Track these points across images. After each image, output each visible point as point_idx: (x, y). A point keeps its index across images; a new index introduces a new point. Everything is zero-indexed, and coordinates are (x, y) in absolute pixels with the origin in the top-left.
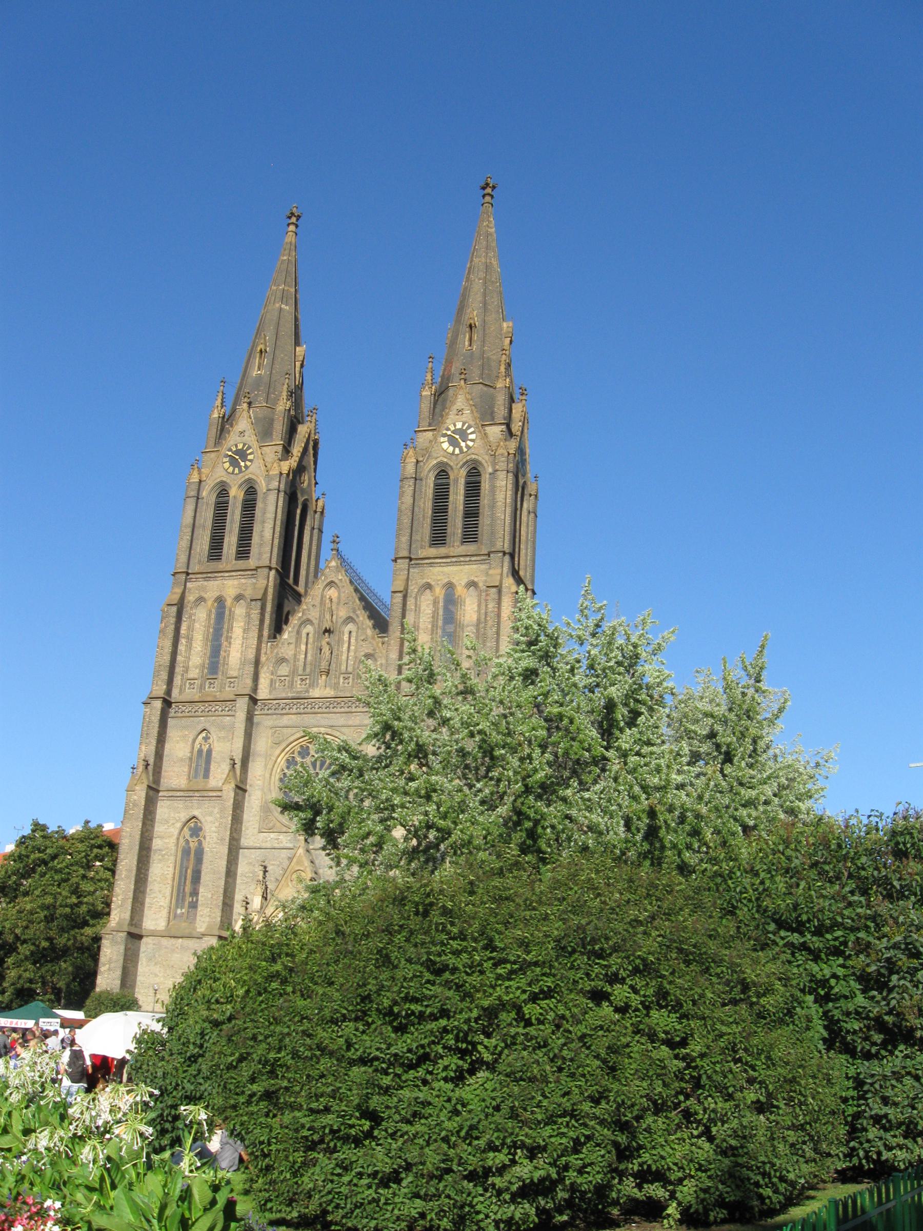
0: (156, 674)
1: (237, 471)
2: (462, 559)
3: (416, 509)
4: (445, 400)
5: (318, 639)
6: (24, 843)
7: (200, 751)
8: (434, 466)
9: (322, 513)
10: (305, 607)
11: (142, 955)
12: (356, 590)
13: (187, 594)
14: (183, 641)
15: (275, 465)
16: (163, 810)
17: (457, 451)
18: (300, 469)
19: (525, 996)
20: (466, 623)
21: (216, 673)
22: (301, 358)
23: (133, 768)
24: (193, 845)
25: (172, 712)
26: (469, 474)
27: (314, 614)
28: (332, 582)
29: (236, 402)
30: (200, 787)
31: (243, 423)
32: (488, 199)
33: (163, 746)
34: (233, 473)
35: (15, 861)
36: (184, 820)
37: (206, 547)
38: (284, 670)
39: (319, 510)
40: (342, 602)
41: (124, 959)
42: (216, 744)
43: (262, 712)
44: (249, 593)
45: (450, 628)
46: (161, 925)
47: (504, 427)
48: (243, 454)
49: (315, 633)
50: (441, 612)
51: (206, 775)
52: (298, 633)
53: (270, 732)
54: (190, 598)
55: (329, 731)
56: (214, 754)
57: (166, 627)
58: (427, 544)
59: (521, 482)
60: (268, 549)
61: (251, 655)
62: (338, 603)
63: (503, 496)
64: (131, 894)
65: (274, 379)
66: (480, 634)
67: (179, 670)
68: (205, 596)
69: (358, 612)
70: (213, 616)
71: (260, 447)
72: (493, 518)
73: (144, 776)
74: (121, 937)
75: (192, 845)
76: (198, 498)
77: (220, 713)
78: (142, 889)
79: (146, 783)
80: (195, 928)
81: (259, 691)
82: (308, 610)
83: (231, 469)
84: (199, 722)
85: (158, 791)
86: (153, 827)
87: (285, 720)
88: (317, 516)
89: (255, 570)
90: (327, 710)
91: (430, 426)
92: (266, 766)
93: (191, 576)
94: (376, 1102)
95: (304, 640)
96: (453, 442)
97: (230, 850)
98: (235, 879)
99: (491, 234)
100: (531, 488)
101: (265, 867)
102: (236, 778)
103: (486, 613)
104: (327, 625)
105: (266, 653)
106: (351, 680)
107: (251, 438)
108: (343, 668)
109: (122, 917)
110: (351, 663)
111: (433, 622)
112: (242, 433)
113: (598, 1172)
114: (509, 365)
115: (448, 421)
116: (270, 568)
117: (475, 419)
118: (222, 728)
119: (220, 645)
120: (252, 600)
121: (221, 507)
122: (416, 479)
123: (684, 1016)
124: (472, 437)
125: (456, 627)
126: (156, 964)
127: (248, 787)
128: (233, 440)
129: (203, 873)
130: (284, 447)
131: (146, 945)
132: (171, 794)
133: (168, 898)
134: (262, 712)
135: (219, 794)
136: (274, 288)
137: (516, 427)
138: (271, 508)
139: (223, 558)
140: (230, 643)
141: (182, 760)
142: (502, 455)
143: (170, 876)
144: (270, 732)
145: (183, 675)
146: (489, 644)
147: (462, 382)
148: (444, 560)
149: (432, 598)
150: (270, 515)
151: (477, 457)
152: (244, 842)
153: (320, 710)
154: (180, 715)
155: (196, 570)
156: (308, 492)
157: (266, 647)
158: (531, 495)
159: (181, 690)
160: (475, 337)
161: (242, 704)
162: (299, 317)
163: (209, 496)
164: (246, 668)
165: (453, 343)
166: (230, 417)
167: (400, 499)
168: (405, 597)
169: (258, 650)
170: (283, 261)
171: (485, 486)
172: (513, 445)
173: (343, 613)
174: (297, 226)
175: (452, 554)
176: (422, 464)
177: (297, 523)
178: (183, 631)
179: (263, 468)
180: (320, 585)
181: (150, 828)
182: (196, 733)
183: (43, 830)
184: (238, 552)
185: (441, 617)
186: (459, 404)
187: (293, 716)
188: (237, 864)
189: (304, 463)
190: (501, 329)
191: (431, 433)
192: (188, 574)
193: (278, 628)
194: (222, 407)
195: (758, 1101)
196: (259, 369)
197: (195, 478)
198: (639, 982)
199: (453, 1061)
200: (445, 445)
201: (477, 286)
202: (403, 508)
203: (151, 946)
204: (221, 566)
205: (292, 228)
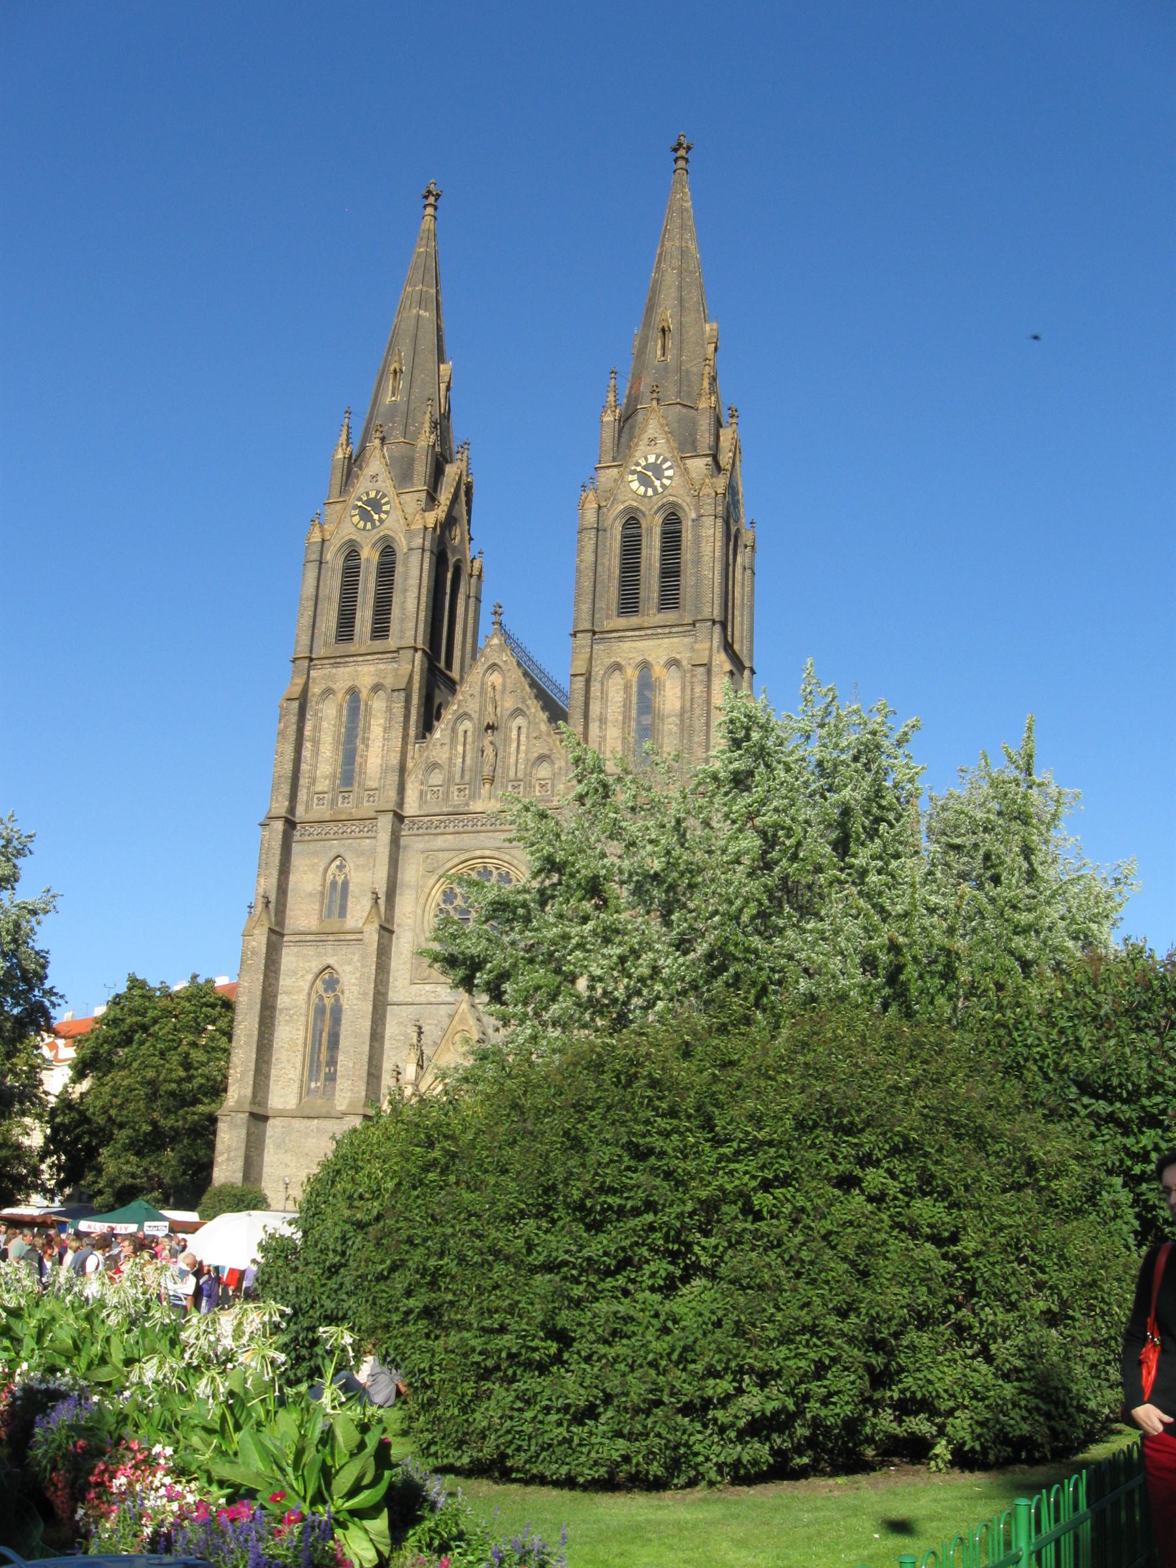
0: (275, 788)
1: (369, 526)
2: (660, 631)
3: (599, 568)
4: (632, 427)
5: (479, 737)
6: (118, 1004)
7: (334, 884)
8: (621, 512)
9: (479, 576)
10: (461, 698)
11: (268, 1141)
12: (526, 674)
13: (311, 685)
14: (308, 745)
15: (418, 517)
16: (289, 958)
17: (650, 492)
18: (450, 522)
19: (754, 1184)
20: (666, 713)
21: (351, 785)
22: (446, 379)
23: (250, 907)
24: (329, 1002)
25: (297, 835)
26: (666, 521)
27: (472, 707)
28: (495, 664)
29: (365, 438)
30: (335, 929)
31: (376, 464)
32: (681, 163)
33: (287, 878)
34: (364, 529)
35: (108, 1025)
36: (316, 970)
37: (333, 625)
38: (437, 778)
39: (476, 572)
40: (509, 689)
41: (247, 1147)
42: (353, 874)
43: (411, 832)
44: (389, 682)
45: (647, 720)
46: (291, 1103)
47: (709, 460)
48: (376, 504)
49: (474, 731)
50: (634, 699)
51: (343, 913)
52: (454, 730)
53: (422, 857)
54: (315, 690)
55: (495, 854)
56: (351, 887)
57: (286, 727)
58: (615, 613)
59: (733, 530)
60: (412, 624)
61: (395, 760)
62: (503, 692)
63: (711, 549)
64: (252, 1066)
65: (412, 406)
66: (686, 729)
67: (303, 781)
68: (335, 687)
69: (529, 702)
70: (345, 712)
71: (398, 495)
72: (698, 575)
73: (264, 916)
74: (241, 1119)
75: (326, 1001)
76: (321, 563)
77: (357, 835)
78: (265, 1058)
79: (267, 925)
80: (333, 1107)
81: (407, 806)
82: (466, 701)
83: (361, 525)
84: (331, 847)
85: (282, 935)
86: (277, 980)
87: (440, 842)
88: (474, 580)
90: (493, 828)
91: (614, 460)
92: (417, 899)
93: (315, 662)
94: (564, 1319)
95: (461, 739)
96: (645, 481)
97: (375, 1006)
98: (382, 1044)
99: (687, 210)
100: (747, 537)
101: (420, 1028)
102: (380, 917)
103: (692, 699)
104: (490, 720)
105: (413, 758)
106: (521, 789)
107: (386, 484)
108: (512, 774)
109: (242, 1093)
110: (521, 766)
111: (624, 712)
112: (374, 477)
113: (847, 1403)
114: (714, 379)
115: (637, 454)
116: (416, 650)
117: (671, 450)
118: (360, 853)
119: (355, 749)
120: (393, 691)
121: (351, 572)
122: (598, 530)
123: (955, 1205)
124: (669, 473)
125: (654, 718)
126: (286, 1151)
127: (395, 928)
128: (364, 487)
129: (342, 1037)
130: (428, 493)
131: (273, 1128)
132: (298, 938)
133: (299, 1068)
134: (411, 832)
135: (359, 936)
136: (409, 289)
137: (725, 459)
138: (414, 572)
139: (356, 638)
140: (367, 746)
141: (311, 895)
142: (708, 495)
143: (300, 1042)
144: (422, 857)
145: (309, 788)
146: (696, 739)
147: (655, 402)
148: (637, 633)
149: (622, 682)
150: (413, 582)
151: (674, 499)
152: (392, 996)
153: (484, 828)
154: (307, 838)
156: (459, 549)
157: (413, 750)
158: (746, 546)
159: (307, 806)
160: (670, 344)
161: (386, 822)
162: (443, 326)
163: (335, 559)
164: (389, 778)
165: (642, 351)
166: (358, 456)
167: (579, 556)
168: (588, 682)
169: (404, 753)
170: (419, 254)
171: (687, 536)
172: (721, 482)
173: (509, 704)
174: (436, 208)
175: (646, 625)
176: (605, 510)
177: (448, 590)
178: (308, 732)
179: (402, 521)
180: (480, 668)
181: (273, 982)
182: (328, 860)
183: (142, 988)
185: (634, 706)
186: (650, 431)
187: (449, 837)
188: (384, 1024)
189: (454, 514)
190: (703, 332)
191: (615, 470)
192: (311, 659)
193: (427, 727)
194: (348, 445)
195: (1049, 1311)
196: (393, 394)
197: (316, 537)
198: (897, 1165)
199: (662, 1267)
200: (635, 485)
201: (670, 278)
202: (582, 567)
203: (279, 1129)
204: (352, 648)
205: (430, 210)
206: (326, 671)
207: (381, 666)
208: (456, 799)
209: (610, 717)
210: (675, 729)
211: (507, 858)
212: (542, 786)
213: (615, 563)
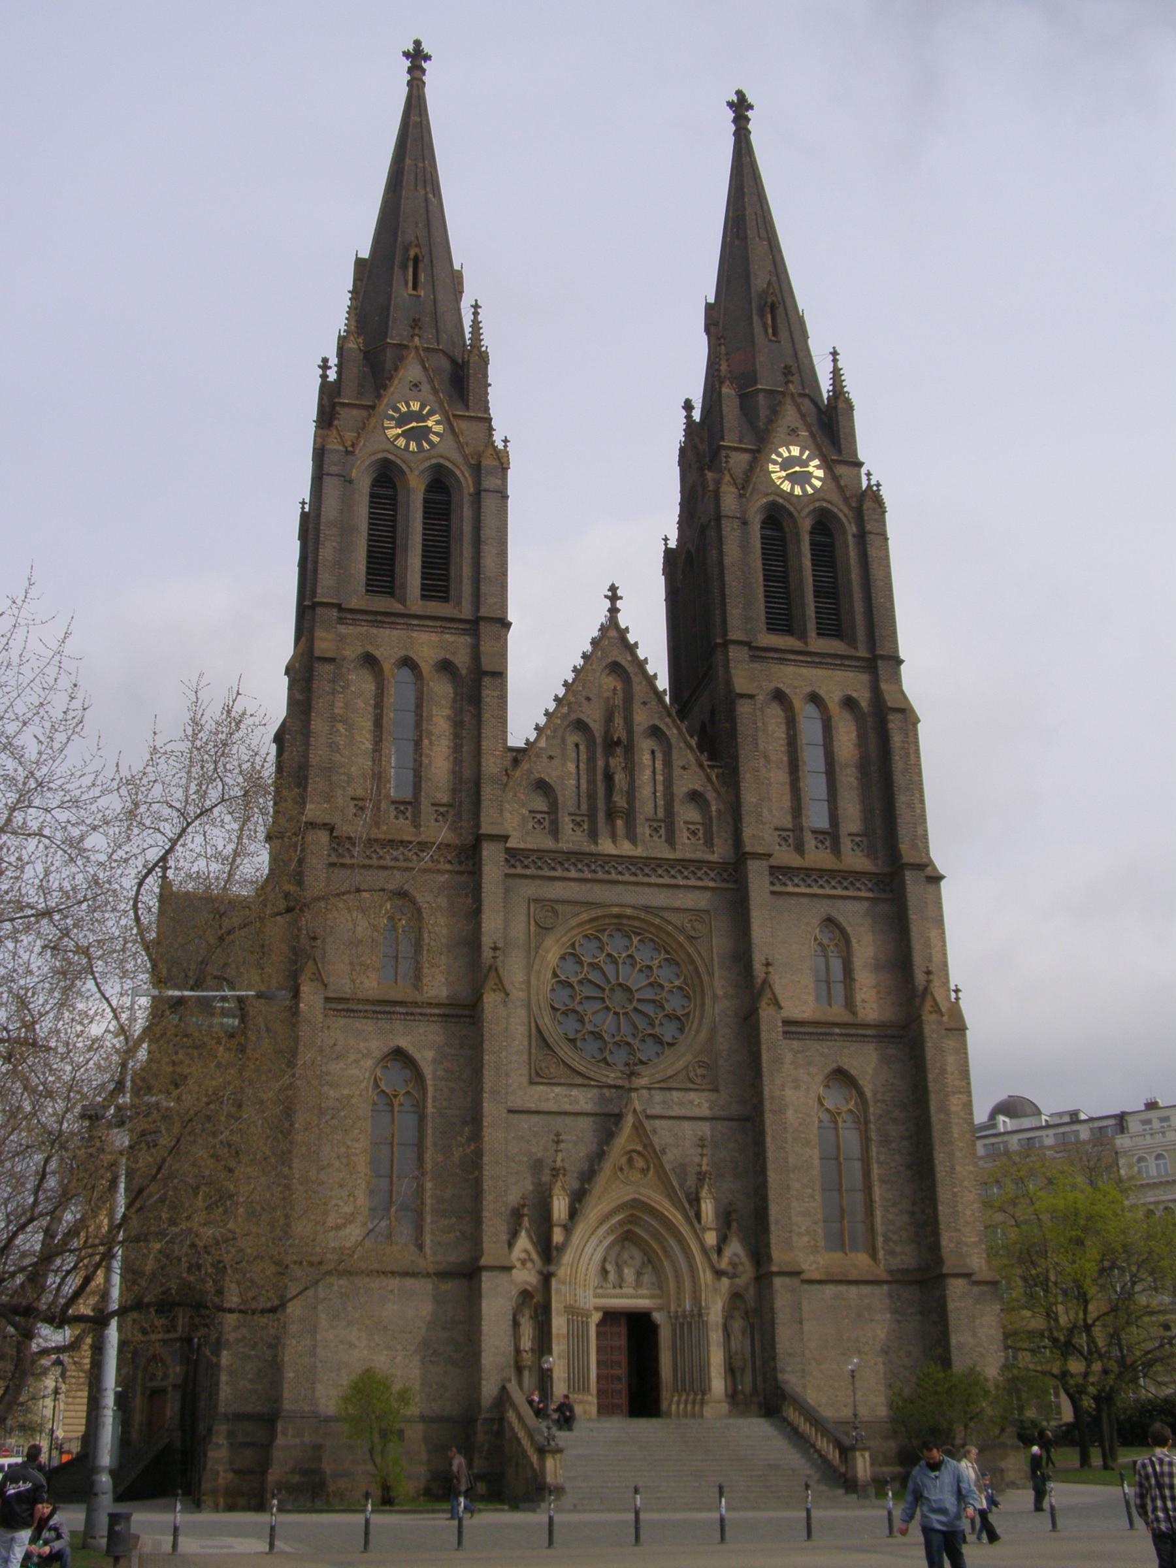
2: (830, 661)
10: (573, 699)
14: (341, 727)
36: (377, 1054)
38: (540, 804)
55: (643, 915)
58: (764, 627)
68: (377, 654)
87: (557, 890)
90: (633, 879)
91: (741, 442)
106: (662, 831)
140: (431, 743)
142: (874, 509)
148: (800, 658)
151: (829, 506)
155: (352, 606)
184: (424, 588)
187: (572, 884)
191: (745, 458)
196: (415, 288)
206: (359, 629)
207: (447, 636)
211: (657, 921)
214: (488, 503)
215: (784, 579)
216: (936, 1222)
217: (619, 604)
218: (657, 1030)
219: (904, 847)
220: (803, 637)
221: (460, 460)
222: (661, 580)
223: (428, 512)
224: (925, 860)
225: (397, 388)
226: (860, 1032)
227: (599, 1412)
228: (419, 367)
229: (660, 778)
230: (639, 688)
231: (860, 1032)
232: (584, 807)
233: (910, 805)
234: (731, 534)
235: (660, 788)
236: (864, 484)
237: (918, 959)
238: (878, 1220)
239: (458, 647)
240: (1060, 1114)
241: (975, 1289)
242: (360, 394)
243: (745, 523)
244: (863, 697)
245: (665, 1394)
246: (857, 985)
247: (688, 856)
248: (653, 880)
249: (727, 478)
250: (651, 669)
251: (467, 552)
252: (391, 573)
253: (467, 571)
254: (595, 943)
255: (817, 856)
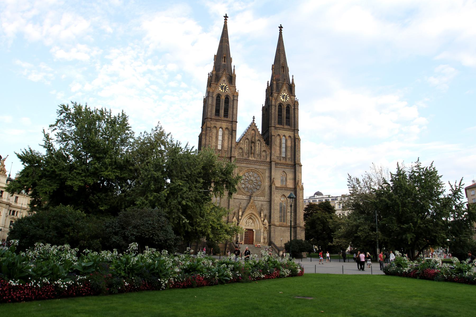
14: (211, 138)
38: (241, 151)
55: (255, 169)
68: (217, 126)
87: (242, 165)
89: (232, 121)
104: (254, 141)
112: (224, 81)
115: (282, 92)
117: (289, 93)
173: (257, 138)
184: (224, 115)
191: (277, 94)
200: (281, 98)
208: (245, 156)
209: (277, 145)
210: (290, 150)
211: (257, 170)
212: (264, 157)
213: (277, 113)
214: (235, 102)
215: (281, 115)
216: (296, 219)
217: (255, 119)
218: (256, 187)
219: (296, 161)
220: (283, 125)
221: (231, 94)
222: (261, 112)
223: (225, 103)
224: (299, 163)
225: (221, 81)
226: (287, 189)
227: (244, 244)
228: (225, 78)
229: (259, 148)
230: (257, 134)
231: (287, 189)
232: (247, 152)
233: (298, 154)
234: (273, 108)
235: (259, 149)
236: (296, 100)
237: (297, 179)
238: (288, 218)
239: (229, 125)
240: (327, 195)
241: (301, 229)
242: (215, 82)
243: (275, 106)
244: (292, 136)
245: (254, 242)
246: (287, 182)
247: (263, 160)
248: (257, 164)
249: (273, 99)
250: (259, 130)
251: (231, 110)
252: (219, 113)
253: (231, 113)
254: (248, 173)
255: (283, 161)
